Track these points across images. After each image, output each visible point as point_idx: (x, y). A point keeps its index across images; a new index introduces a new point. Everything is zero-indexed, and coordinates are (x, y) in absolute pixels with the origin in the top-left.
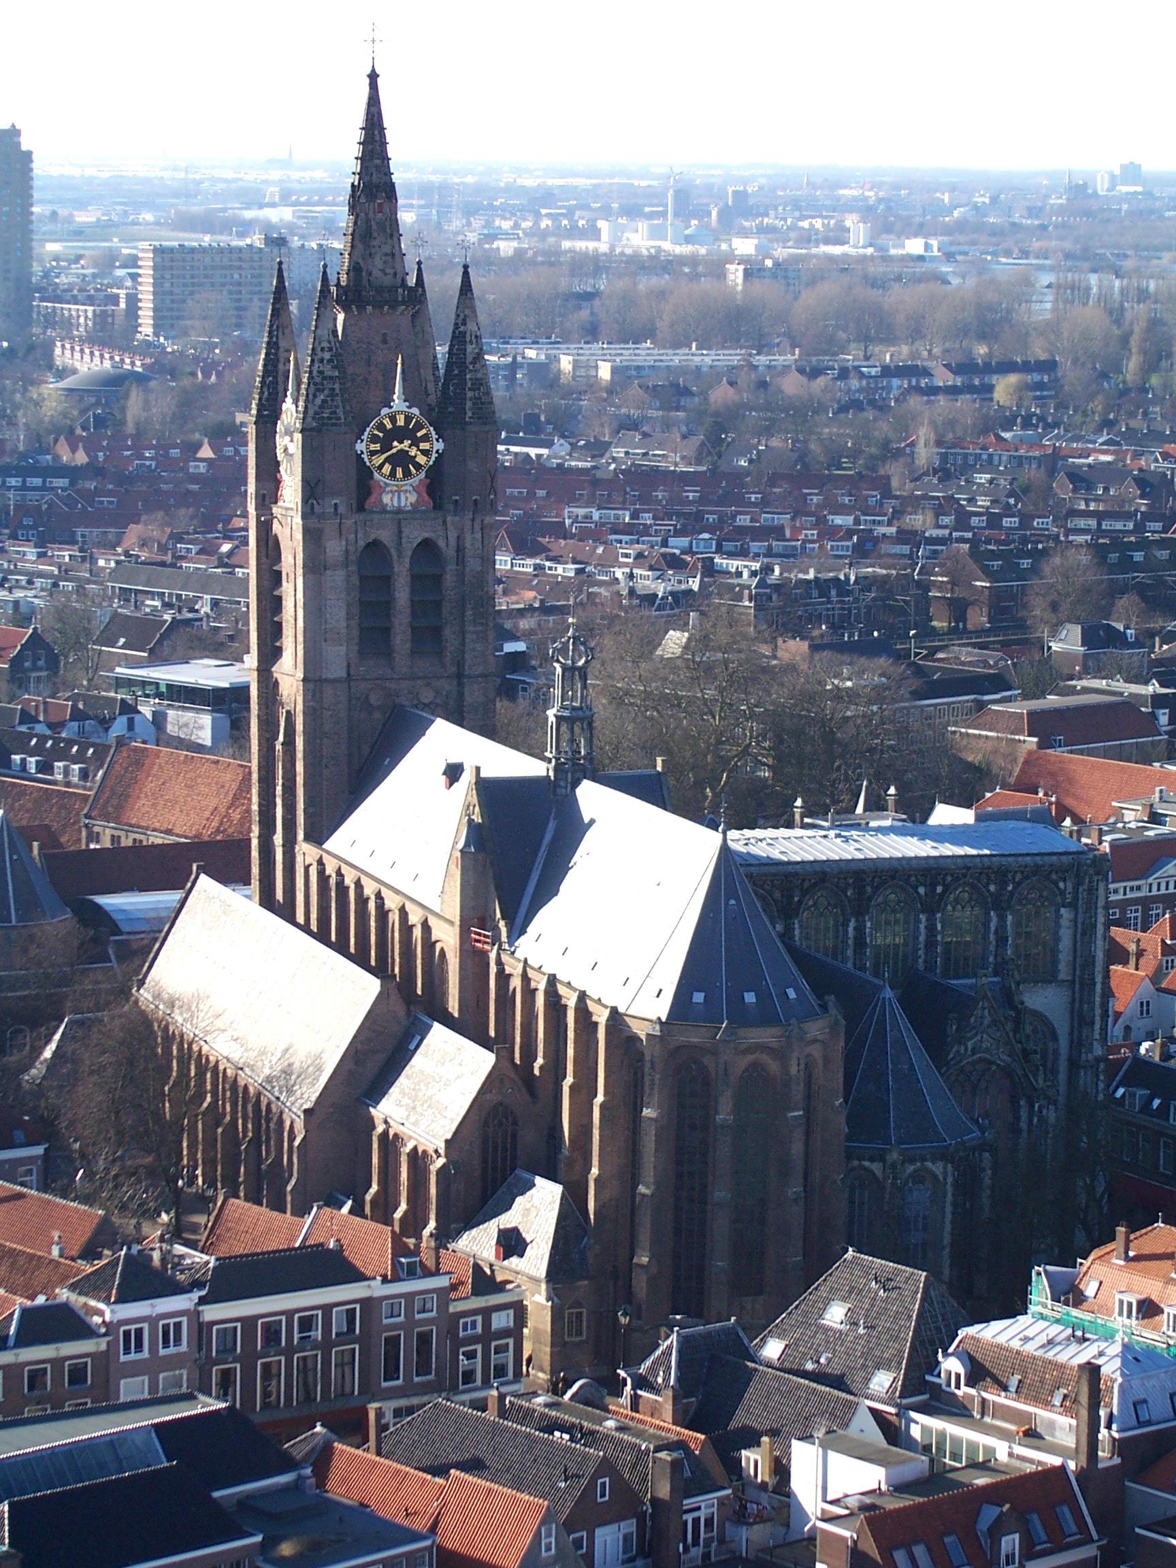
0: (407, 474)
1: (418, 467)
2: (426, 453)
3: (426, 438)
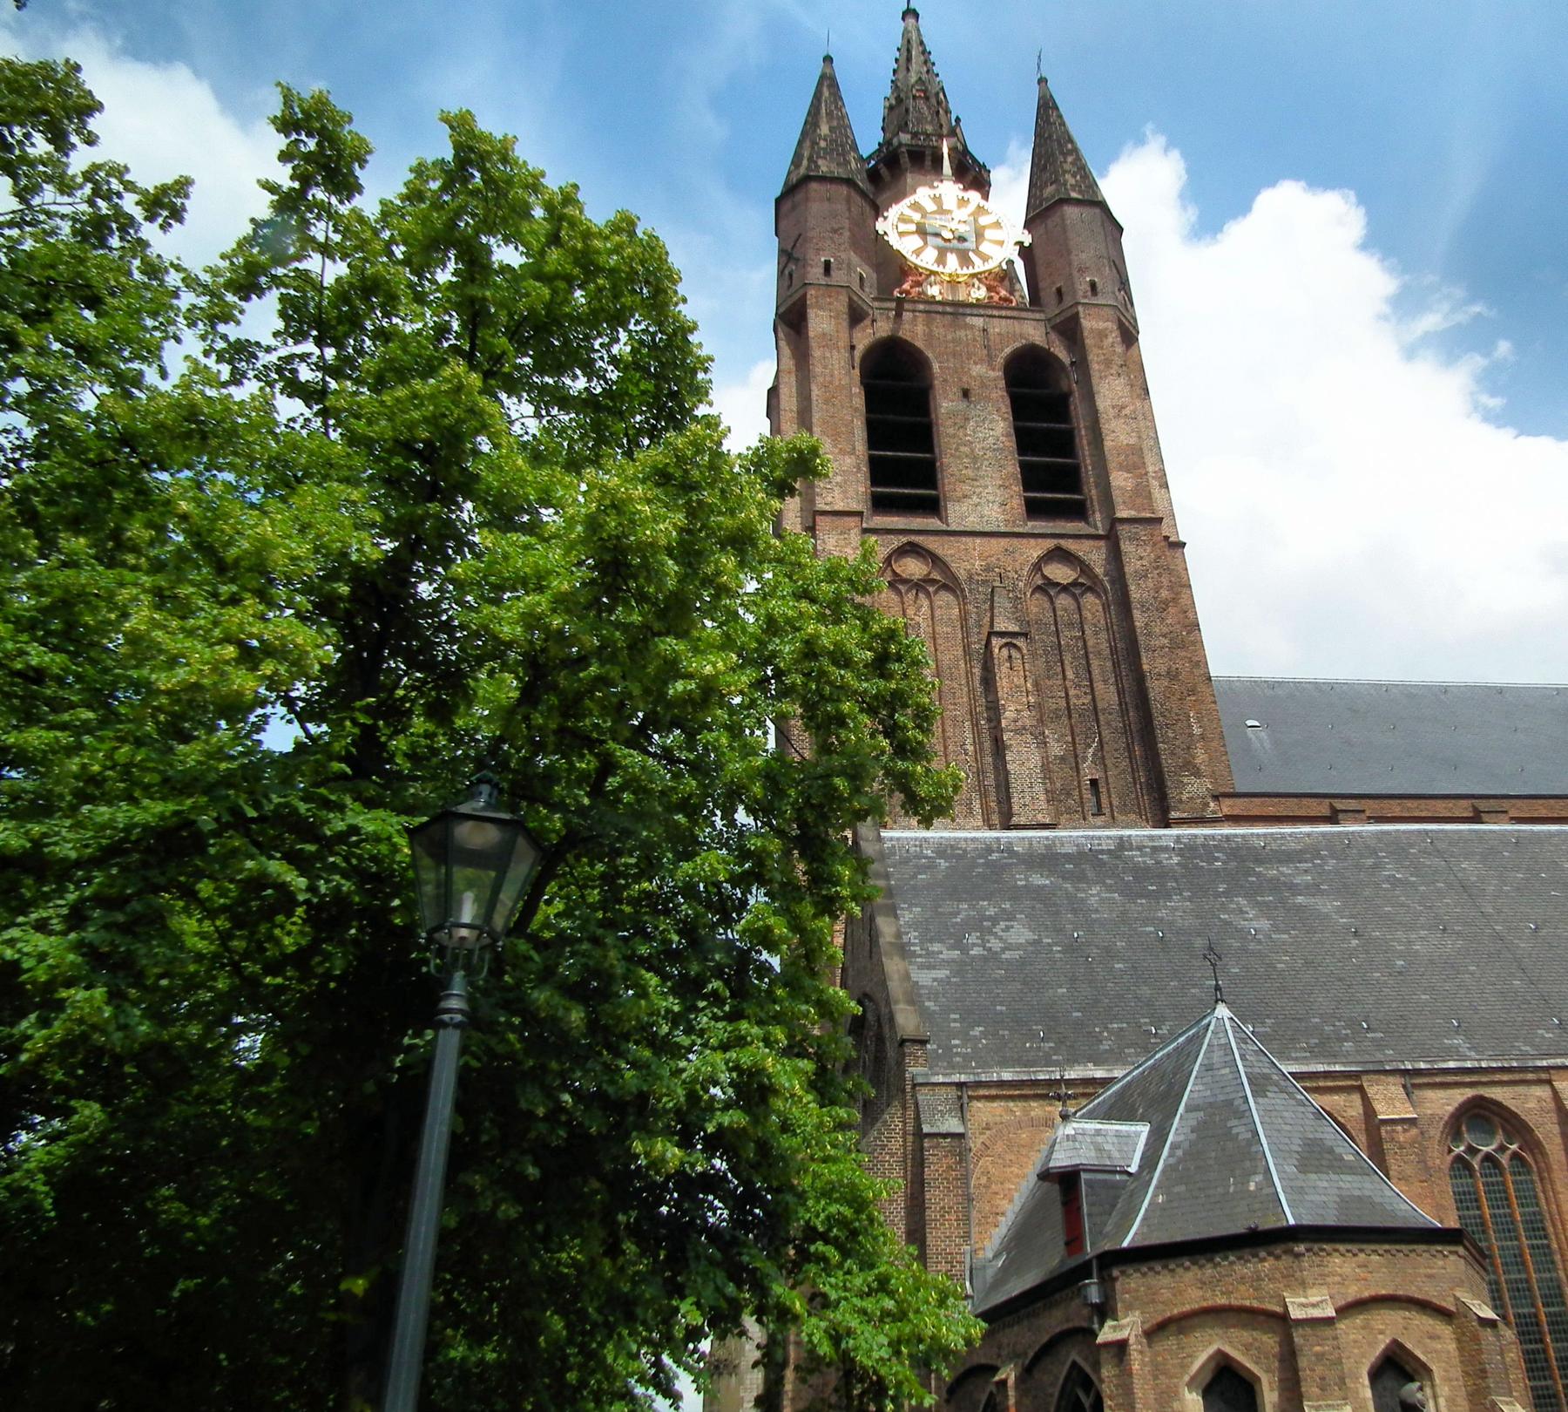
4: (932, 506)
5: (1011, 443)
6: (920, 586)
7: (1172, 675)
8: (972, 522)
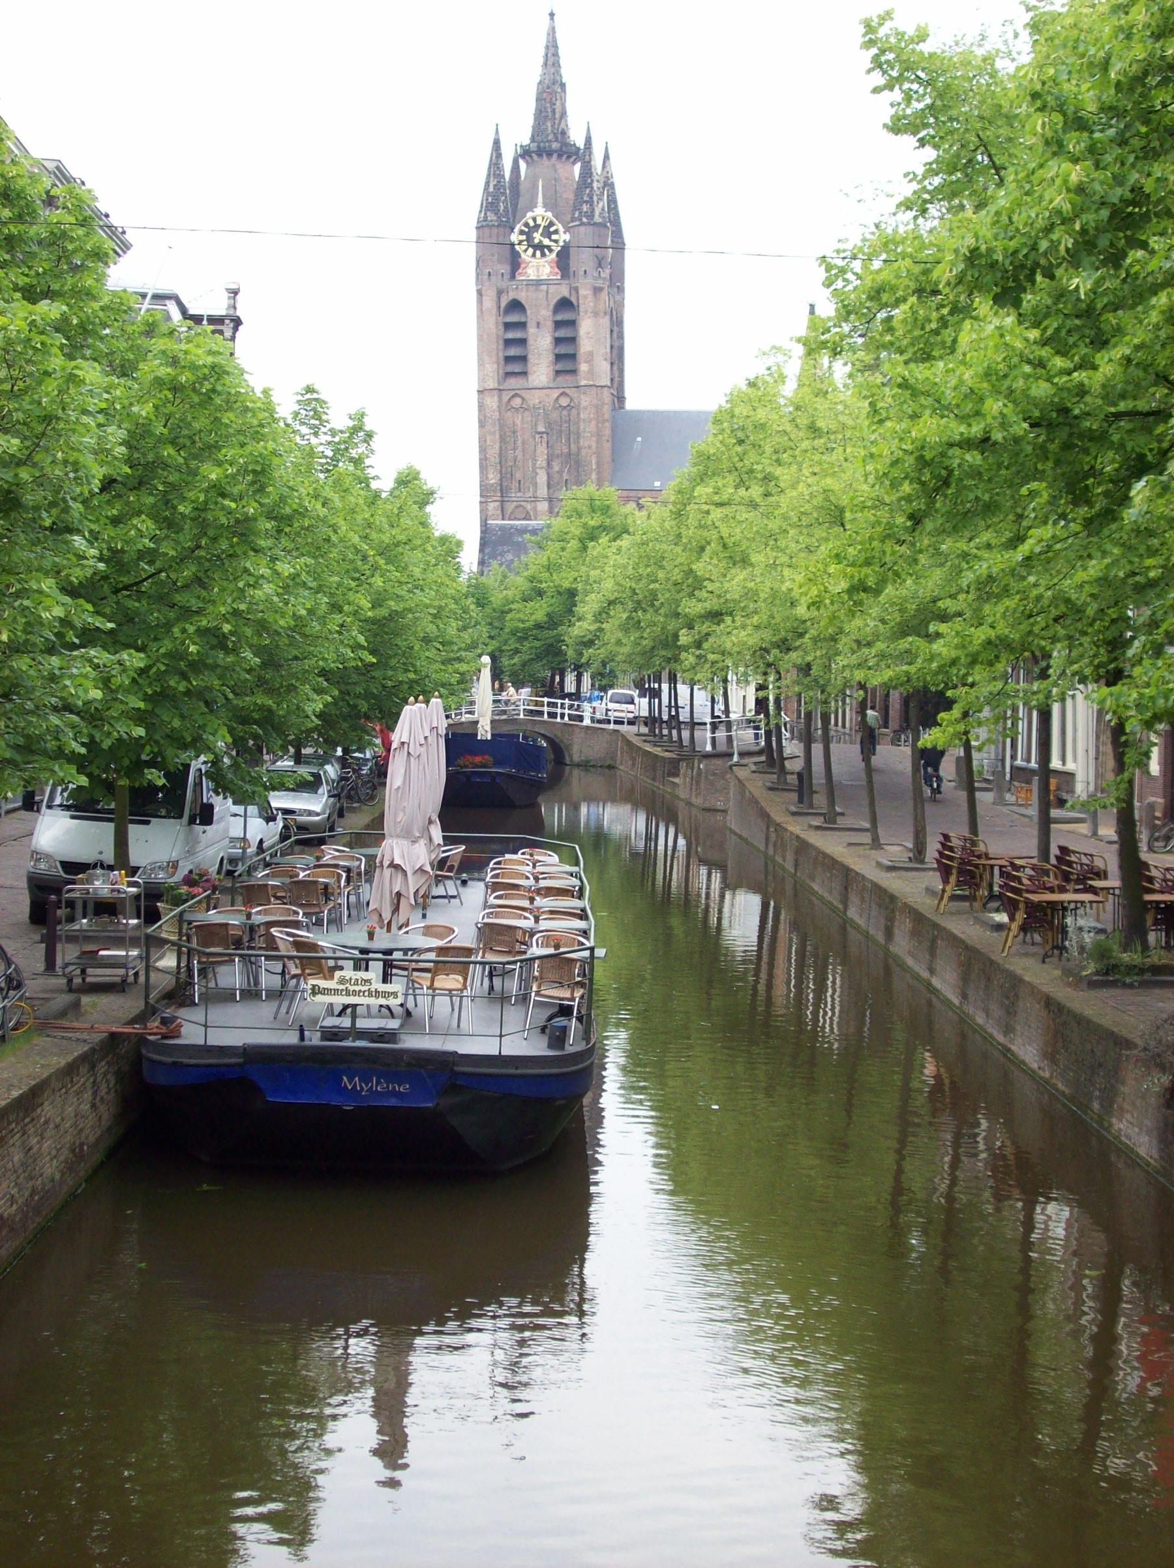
0: (543, 255)
2: (556, 241)
3: (556, 232)
4: (524, 374)
6: (517, 410)
7: (589, 447)
8: (536, 383)
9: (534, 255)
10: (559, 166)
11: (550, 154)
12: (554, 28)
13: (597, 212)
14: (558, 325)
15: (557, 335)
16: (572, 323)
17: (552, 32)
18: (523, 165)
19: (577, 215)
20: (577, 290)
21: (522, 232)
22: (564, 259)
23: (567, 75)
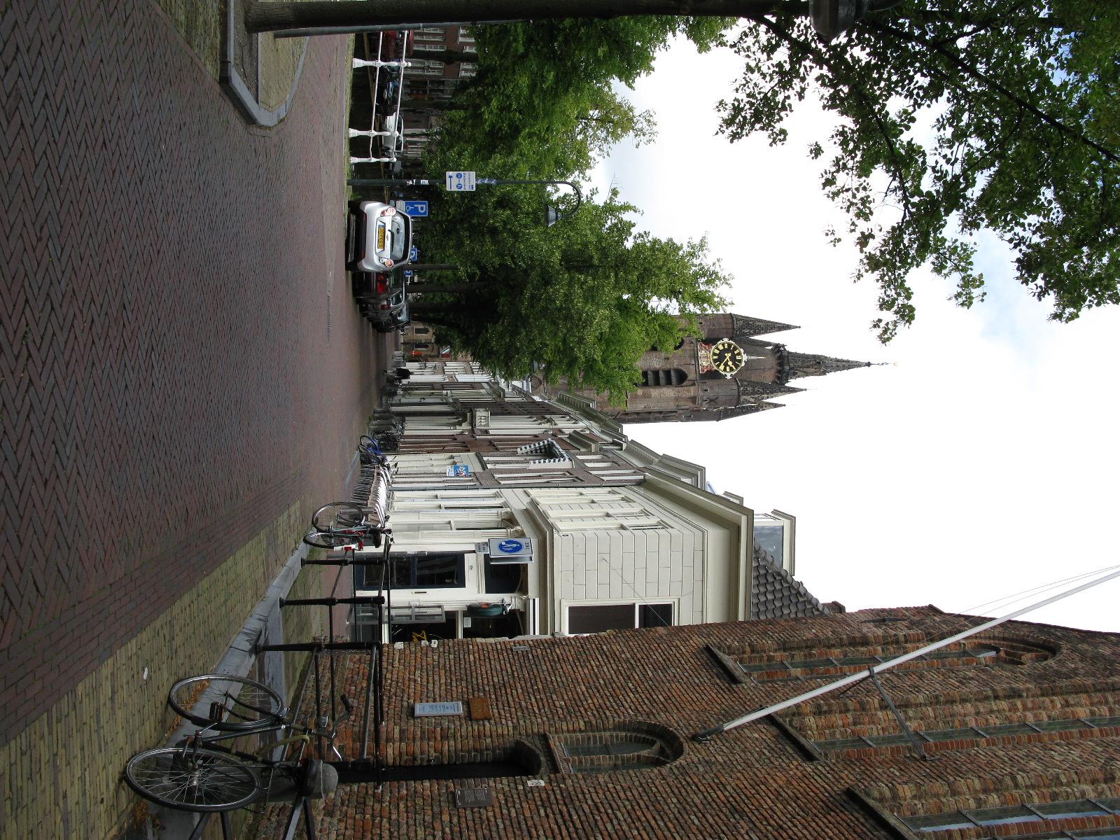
0: (715, 361)
1: (718, 366)
5: (652, 368)
9: (714, 354)
10: (773, 371)
11: (781, 364)
12: (860, 366)
13: (748, 398)
14: (668, 373)
15: (661, 372)
16: (669, 383)
17: (856, 365)
18: (770, 348)
19: (746, 383)
20: (694, 384)
21: (730, 345)
22: (713, 375)
23: (832, 376)
